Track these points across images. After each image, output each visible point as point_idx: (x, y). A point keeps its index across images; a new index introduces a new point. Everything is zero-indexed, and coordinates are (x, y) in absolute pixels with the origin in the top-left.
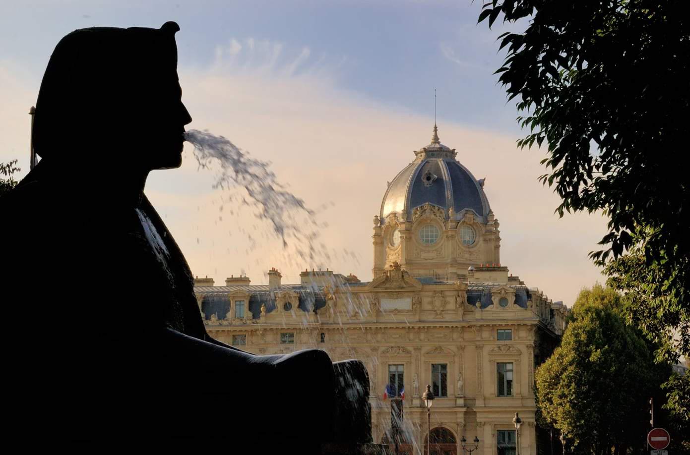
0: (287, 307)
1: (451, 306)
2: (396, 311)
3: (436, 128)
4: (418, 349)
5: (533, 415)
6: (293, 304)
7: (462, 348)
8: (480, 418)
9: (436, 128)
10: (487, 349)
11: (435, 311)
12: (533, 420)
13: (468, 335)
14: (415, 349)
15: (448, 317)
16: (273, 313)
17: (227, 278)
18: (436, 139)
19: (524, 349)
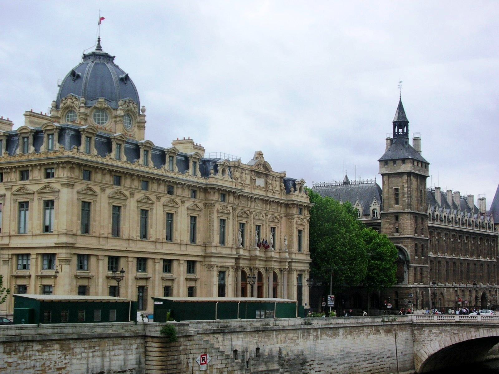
0: (223, 171)
1: (278, 188)
2: (259, 187)
3: (99, 39)
4: (266, 215)
5: (308, 265)
6: (226, 170)
7: (281, 218)
8: (294, 266)
9: (99, 39)
10: (296, 219)
11: (273, 190)
12: (308, 268)
13: (283, 210)
14: (265, 215)
15: (277, 196)
16: (217, 176)
17: (173, 141)
18: (99, 47)
19: (305, 220)
